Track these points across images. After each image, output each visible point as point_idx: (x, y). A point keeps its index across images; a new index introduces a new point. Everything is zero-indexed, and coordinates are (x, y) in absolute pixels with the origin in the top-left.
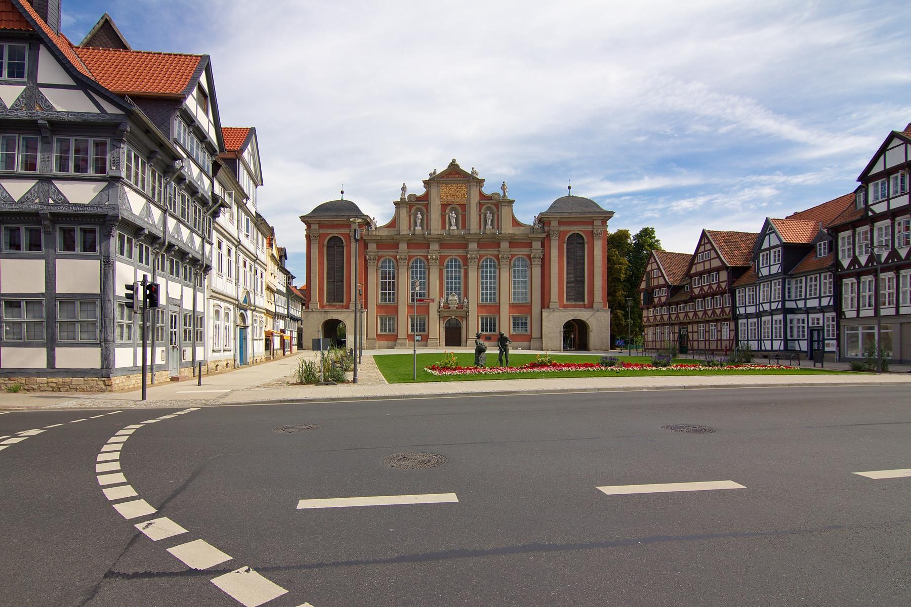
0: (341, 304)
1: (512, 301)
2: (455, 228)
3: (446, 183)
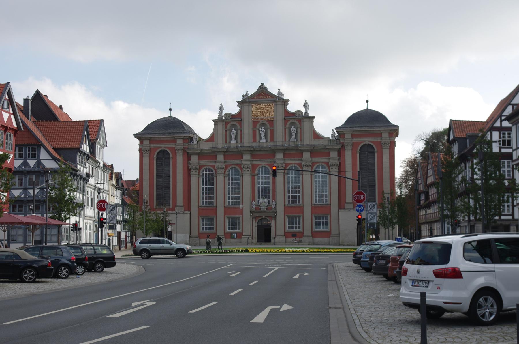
0: (168, 207)
1: (314, 202)
2: (264, 141)
3: (257, 103)
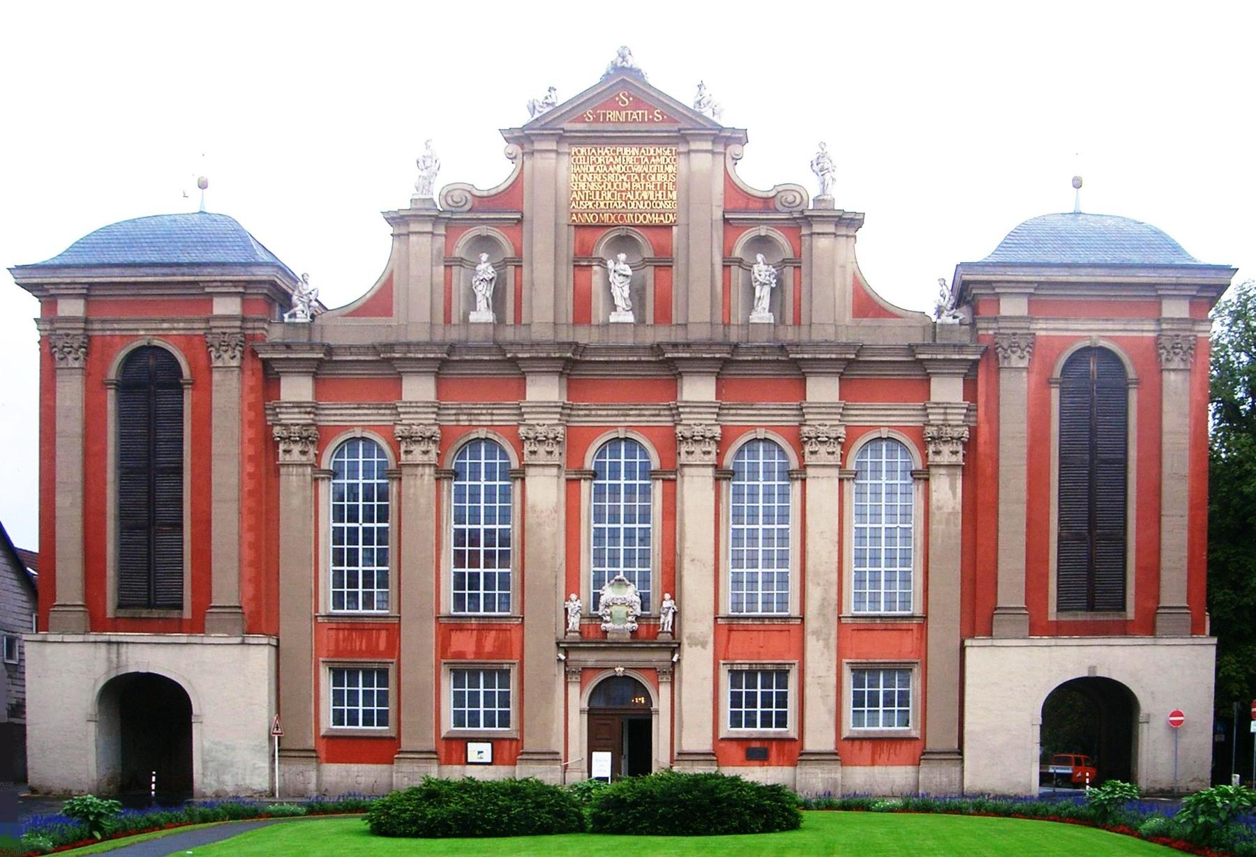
1: (850, 609)
2: (630, 318)
